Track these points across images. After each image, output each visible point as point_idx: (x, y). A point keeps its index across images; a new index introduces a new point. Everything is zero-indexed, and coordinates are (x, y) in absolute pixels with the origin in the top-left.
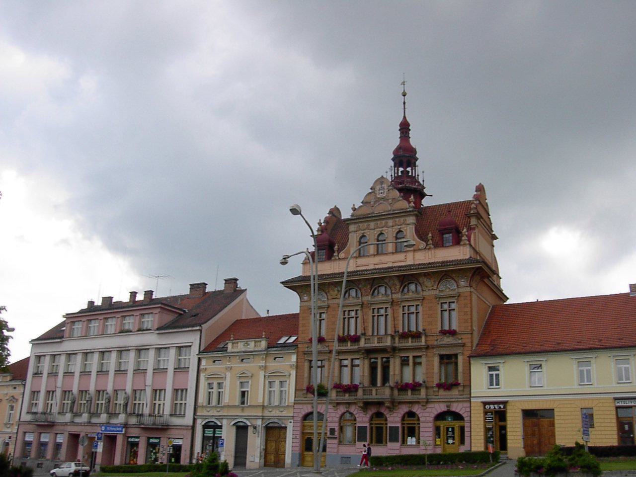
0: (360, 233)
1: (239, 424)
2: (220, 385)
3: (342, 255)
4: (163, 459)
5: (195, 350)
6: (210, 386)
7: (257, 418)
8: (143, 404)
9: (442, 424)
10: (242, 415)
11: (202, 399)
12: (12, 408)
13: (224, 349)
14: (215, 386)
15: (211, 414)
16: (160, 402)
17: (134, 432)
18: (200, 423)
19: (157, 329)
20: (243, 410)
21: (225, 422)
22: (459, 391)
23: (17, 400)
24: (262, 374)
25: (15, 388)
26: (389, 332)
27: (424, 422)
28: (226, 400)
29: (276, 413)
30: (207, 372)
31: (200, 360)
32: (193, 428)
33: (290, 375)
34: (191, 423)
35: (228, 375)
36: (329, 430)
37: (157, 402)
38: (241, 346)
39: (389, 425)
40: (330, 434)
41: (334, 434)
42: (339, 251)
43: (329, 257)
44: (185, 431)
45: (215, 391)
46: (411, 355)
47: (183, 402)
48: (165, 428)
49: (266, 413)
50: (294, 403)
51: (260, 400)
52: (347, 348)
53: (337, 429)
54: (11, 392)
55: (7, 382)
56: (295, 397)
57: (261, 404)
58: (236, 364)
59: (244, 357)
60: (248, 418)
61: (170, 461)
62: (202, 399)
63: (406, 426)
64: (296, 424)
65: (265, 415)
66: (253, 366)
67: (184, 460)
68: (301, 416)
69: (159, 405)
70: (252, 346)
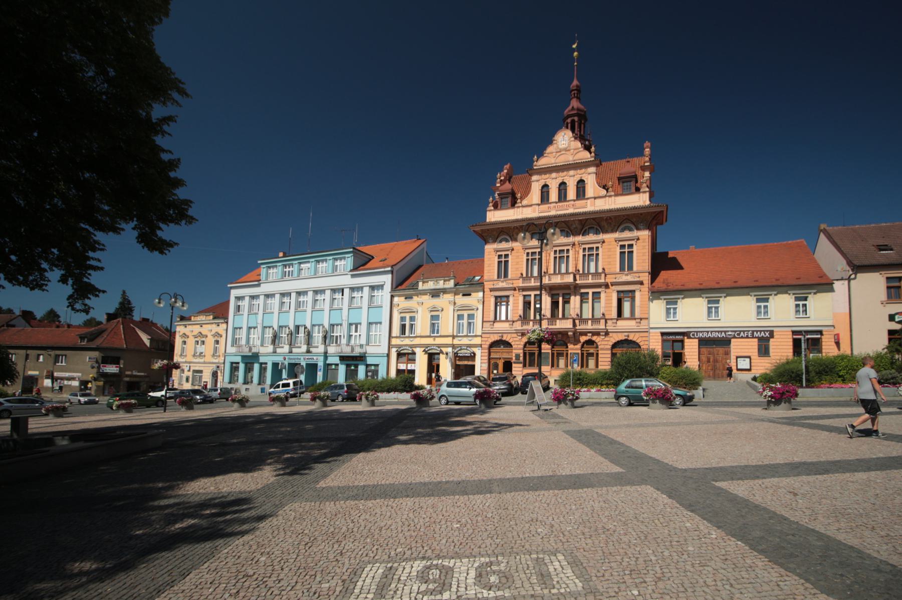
0: (542, 183)
1: (430, 351)
2: (412, 319)
3: (525, 202)
5: (388, 287)
6: (403, 319)
7: (447, 346)
8: (340, 336)
9: (618, 351)
11: (396, 331)
12: (217, 342)
16: (356, 334)
17: (332, 360)
19: (351, 271)
20: (434, 340)
21: (419, 351)
22: (637, 322)
23: (221, 336)
24: (452, 308)
25: (218, 325)
26: (570, 270)
27: (602, 349)
28: (418, 330)
29: (465, 341)
30: (399, 307)
31: (392, 297)
32: (388, 355)
33: (477, 309)
34: (387, 352)
35: (420, 309)
36: (514, 355)
38: (431, 285)
39: (570, 352)
40: (516, 359)
41: (519, 360)
42: (522, 198)
43: (513, 204)
46: (590, 291)
47: (378, 333)
49: (456, 342)
50: (482, 333)
51: (450, 332)
52: (530, 285)
53: (522, 355)
54: (215, 328)
55: (210, 320)
56: (482, 327)
57: (451, 334)
58: (426, 298)
59: (435, 293)
60: (439, 346)
63: (585, 352)
64: (483, 351)
65: (454, 343)
66: (444, 301)
68: (488, 343)
69: (356, 336)
70: (441, 284)
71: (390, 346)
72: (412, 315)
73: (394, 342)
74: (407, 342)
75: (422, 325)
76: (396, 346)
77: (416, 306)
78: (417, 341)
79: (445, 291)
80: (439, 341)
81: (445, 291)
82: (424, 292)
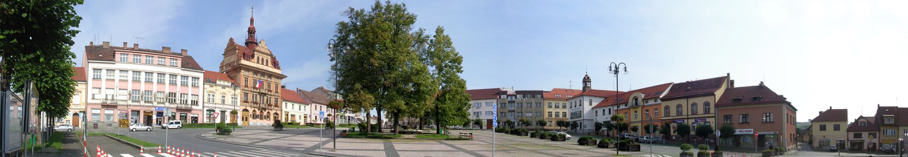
2: (213, 96)
4: (189, 121)
10: (224, 107)
11: (206, 100)
13: (215, 82)
14: (211, 95)
15: (211, 106)
18: (205, 109)
35: (217, 92)
37: (173, 98)
38: (222, 83)
44: (200, 112)
45: (211, 97)
48: (190, 110)
58: (219, 88)
59: (224, 87)
61: (192, 122)
62: (206, 100)
66: (227, 90)
67: (200, 121)
71: (203, 107)
72: (213, 94)
73: (205, 105)
74: (211, 105)
75: (218, 99)
76: (207, 107)
77: (215, 91)
78: (217, 106)
79: (228, 87)
80: (225, 106)
81: (228, 87)
82: (219, 85)
